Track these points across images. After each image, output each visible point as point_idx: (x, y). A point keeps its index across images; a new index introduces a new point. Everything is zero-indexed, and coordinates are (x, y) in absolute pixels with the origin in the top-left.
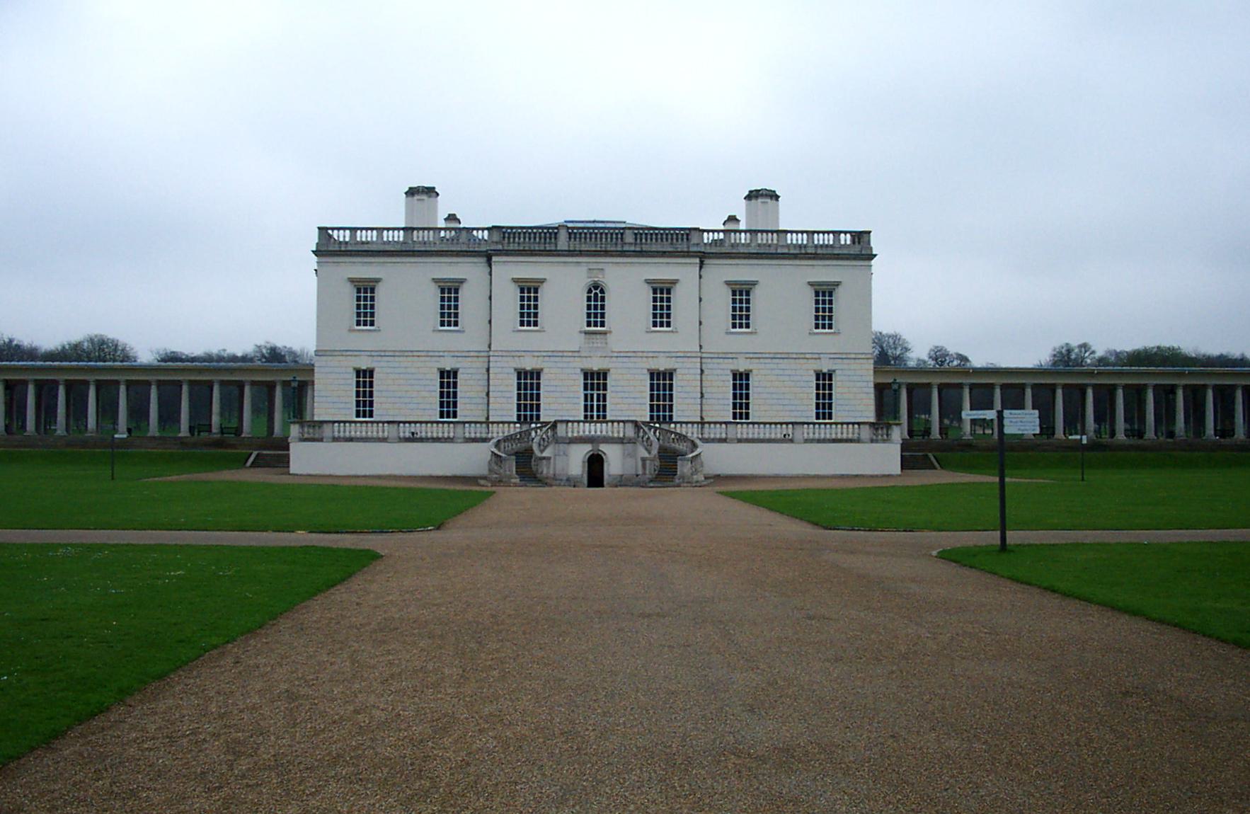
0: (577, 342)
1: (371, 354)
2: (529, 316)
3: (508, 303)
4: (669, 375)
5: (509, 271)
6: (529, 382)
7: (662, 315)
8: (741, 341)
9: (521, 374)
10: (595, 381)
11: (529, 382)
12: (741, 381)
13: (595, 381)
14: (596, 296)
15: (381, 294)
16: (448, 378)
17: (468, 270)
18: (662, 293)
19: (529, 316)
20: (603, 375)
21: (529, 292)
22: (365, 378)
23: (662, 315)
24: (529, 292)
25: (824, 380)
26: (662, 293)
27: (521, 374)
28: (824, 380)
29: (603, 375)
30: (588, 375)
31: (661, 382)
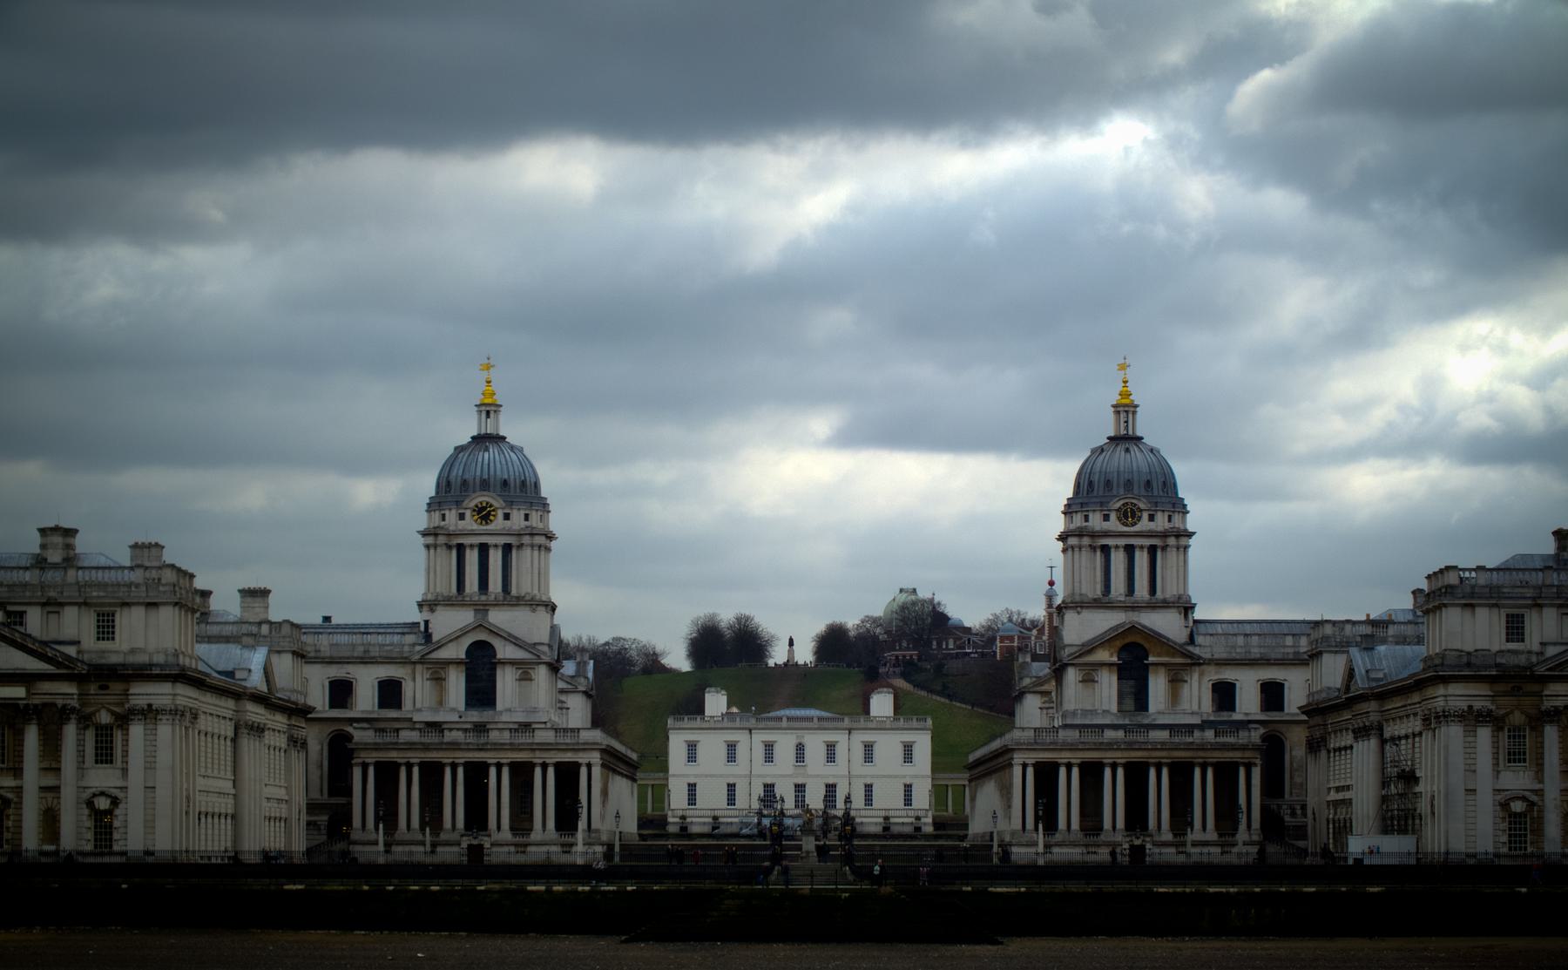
0: (790, 771)
1: (696, 776)
2: (769, 757)
3: (759, 752)
4: (834, 786)
5: (760, 738)
6: (769, 788)
7: (831, 756)
8: (868, 770)
9: (766, 786)
10: (800, 788)
11: (769, 788)
12: (869, 788)
13: (800, 788)
14: (800, 749)
15: (699, 748)
16: (731, 788)
17: (741, 737)
18: (831, 749)
19: (769, 757)
20: (803, 786)
21: (769, 748)
22: (692, 788)
23: (831, 756)
24: (769, 748)
25: (908, 789)
26: (831, 749)
27: (766, 786)
28: (908, 789)
29: (803, 786)
30: (797, 786)
31: (831, 789)
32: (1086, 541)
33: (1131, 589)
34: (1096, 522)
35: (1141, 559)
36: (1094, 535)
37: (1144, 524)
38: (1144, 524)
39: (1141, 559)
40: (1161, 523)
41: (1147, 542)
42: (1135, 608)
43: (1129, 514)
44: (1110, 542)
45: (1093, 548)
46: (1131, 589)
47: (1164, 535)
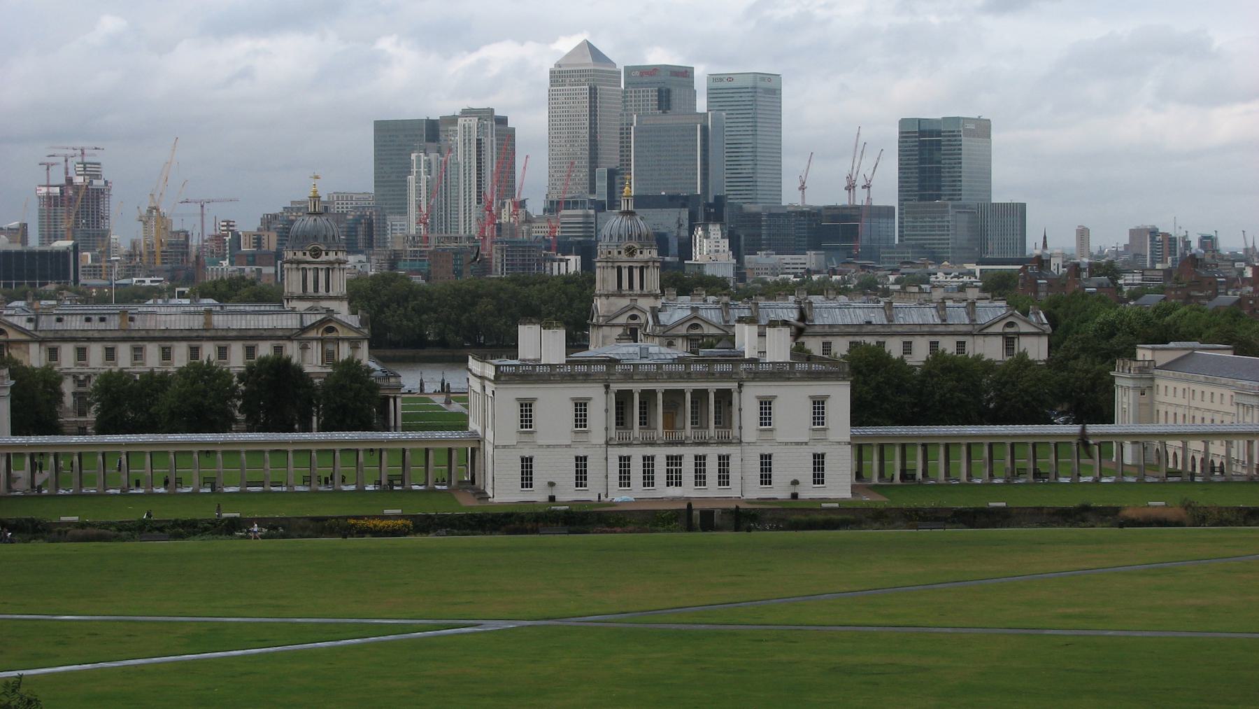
32: (294, 266)
33: (316, 289)
34: (300, 255)
35: (322, 275)
36: (299, 262)
37: (323, 258)
38: (323, 258)
39: (322, 275)
40: (332, 256)
41: (324, 266)
42: (320, 298)
43: (316, 253)
44: (307, 266)
45: (298, 269)
46: (316, 289)
47: (331, 263)
